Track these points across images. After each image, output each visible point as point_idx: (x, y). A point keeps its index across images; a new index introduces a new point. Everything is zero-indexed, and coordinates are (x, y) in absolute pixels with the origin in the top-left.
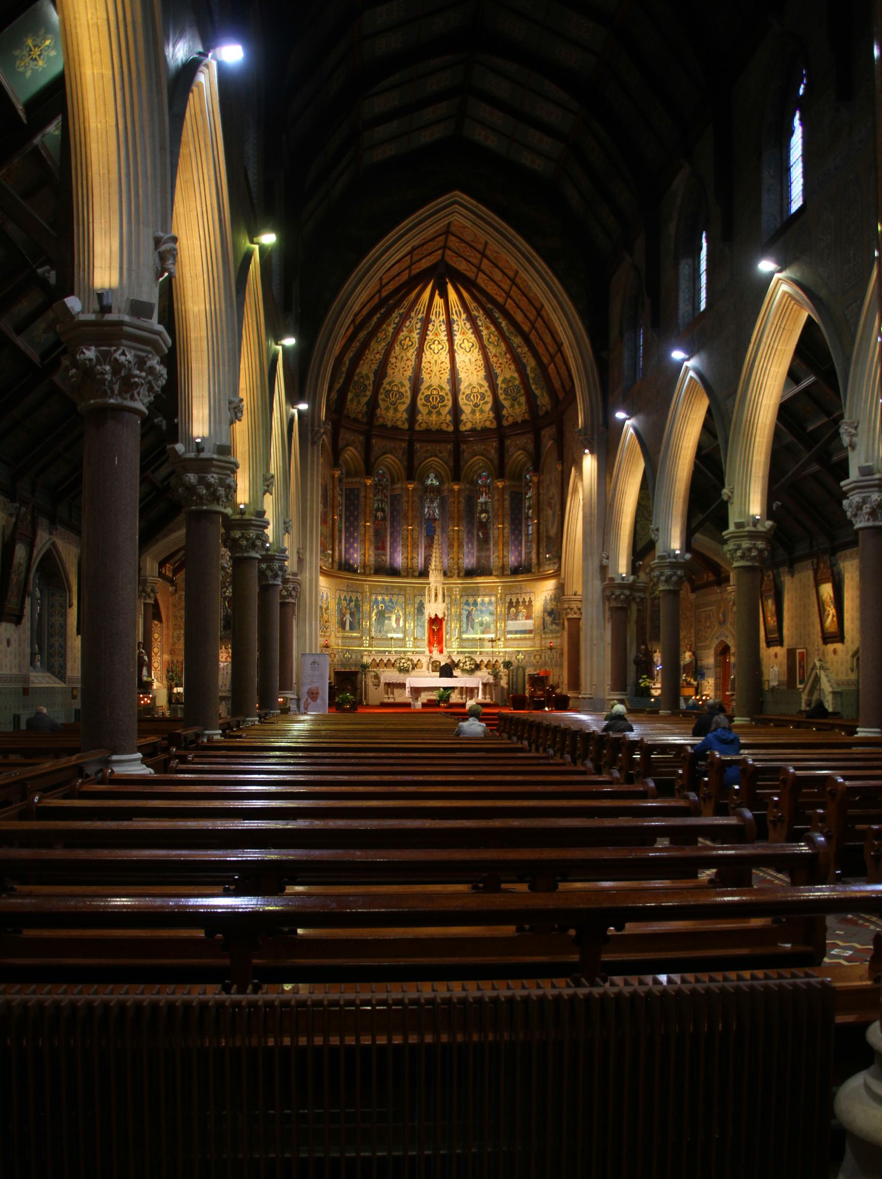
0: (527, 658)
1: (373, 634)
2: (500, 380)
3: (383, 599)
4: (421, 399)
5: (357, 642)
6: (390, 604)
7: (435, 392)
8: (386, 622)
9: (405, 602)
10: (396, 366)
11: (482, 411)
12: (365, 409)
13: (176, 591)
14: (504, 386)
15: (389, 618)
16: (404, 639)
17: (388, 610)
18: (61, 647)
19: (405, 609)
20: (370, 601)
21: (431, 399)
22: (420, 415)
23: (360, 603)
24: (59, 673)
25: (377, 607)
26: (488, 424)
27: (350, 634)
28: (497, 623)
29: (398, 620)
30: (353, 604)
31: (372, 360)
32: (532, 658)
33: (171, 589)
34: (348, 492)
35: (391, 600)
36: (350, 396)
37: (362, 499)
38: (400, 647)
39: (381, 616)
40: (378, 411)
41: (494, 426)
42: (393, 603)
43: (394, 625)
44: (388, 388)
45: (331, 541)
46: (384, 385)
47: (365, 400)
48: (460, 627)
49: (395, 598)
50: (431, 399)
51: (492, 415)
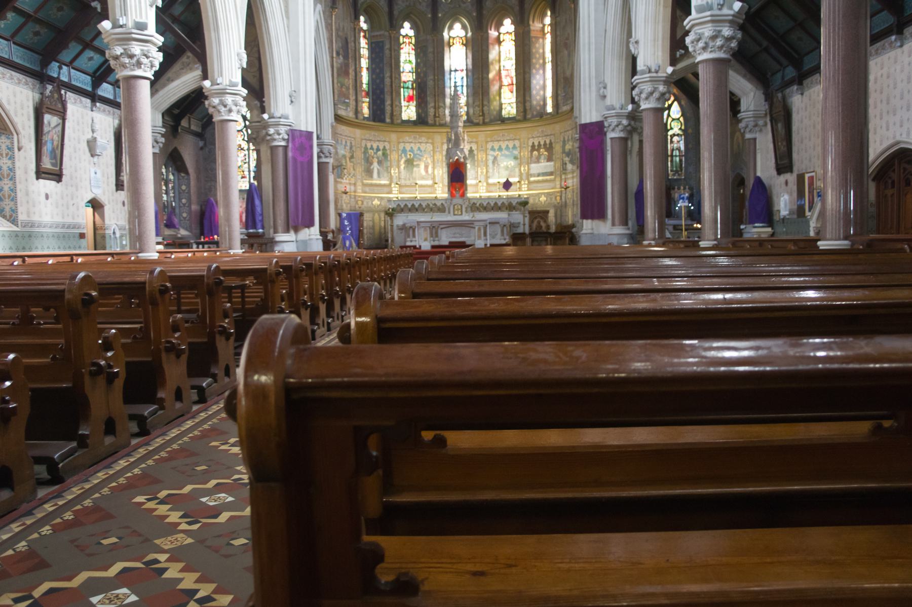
0: (549, 199)
1: (403, 182)
3: (412, 148)
5: (386, 189)
6: (419, 152)
8: (415, 169)
9: (433, 150)
13: (205, 144)
15: (418, 166)
16: (432, 186)
17: (417, 158)
18: (12, 190)
19: (433, 157)
20: (398, 150)
23: (388, 152)
24: (11, 216)
25: (406, 156)
27: (378, 182)
28: (521, 167)
29: (426, 167)
30: (380, 153)
32: (553, 199)
33: (201, 144)
34: (373, 45)
35: (419, 148)
37: (387, 52)
38: (429, 193)
39: (410, 163)
42: (421, 151)
43: (423, 172)
45: (354, 92)
48: (487, 172)
49: (423, 146)
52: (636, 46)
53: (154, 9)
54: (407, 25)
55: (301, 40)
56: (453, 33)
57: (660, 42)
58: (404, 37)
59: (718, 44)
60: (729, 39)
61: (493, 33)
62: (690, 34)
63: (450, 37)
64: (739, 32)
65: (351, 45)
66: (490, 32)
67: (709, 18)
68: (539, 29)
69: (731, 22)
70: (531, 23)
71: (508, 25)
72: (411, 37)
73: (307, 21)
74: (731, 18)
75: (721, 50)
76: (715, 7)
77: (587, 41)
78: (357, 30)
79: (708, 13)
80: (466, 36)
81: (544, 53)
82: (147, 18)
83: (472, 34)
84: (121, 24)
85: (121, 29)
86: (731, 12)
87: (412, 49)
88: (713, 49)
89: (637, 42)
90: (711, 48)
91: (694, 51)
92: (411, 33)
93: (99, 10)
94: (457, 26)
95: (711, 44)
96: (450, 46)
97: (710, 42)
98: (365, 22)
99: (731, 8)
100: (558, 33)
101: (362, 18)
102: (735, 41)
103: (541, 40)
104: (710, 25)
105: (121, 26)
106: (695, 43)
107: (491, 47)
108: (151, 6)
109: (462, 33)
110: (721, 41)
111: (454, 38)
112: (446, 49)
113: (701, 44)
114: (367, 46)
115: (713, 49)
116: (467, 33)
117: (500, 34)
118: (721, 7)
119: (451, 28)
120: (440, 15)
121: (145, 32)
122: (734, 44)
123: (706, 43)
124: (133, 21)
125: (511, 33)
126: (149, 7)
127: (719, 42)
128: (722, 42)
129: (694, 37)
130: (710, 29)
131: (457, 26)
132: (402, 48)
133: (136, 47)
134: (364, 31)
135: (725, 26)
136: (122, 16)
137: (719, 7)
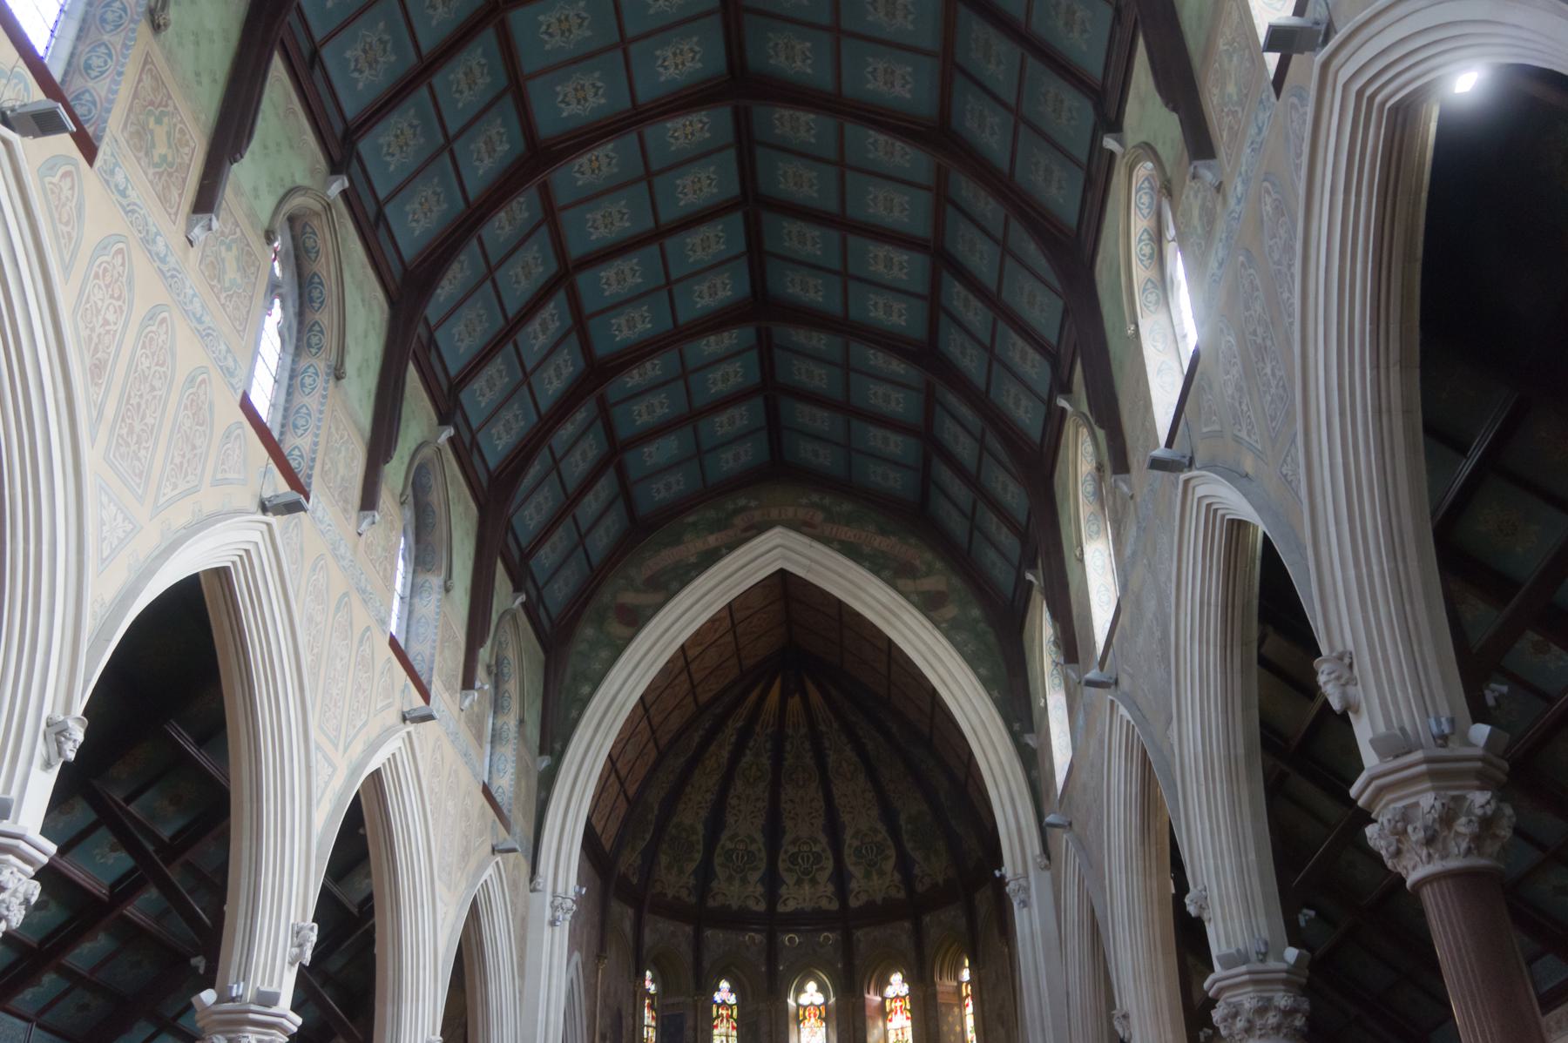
2: (902, 819)
4: (784, 861)
7: (805, 848)
10: (740, 811)
11: (881, 873)
12: (692, 881)
14: (909, 827)
21: (800, 861)
22: (785, 887)
26: (893, 893)
31: (700, 803)
36: (664, 860)
40: (714, 884)
41: (902, 895)
44: (730, 845)
46: (722, 842)
47: (692, 866)
50: (800, 861)
51: (897, 876)
52: (1124, 1023)
53: (295, 969)
54: (724, 985)
55: (541, 1016)
56: (804, 999)
57: (1167, 1016)
58: (719, 1006)
59: (1270, 1022)
60: (1288, 1013)
61: (873, 998)
62: (1217, 1005)
63: (799, 1006)
64: (1304, 999)
65: (627, 1022)
66: (867, 996)
67: (1246, 977)
68: (951, 990)
69: (1285, 982)
70: (937, 979)
71: (897, 985)
72: (731, 1006)
73: (554, 981)
74: (1284, 975)
75: (1278, 1033)
76: (1253, 957)
77: (1036, 1011)
78: (639, 993)
79: (1243, 968)
80: (825, 1003)
81: (963, 1031)
82: (280, 985)
83: (837, 1000)
84: (234, 995)
85: (231, 1004)
86: (1283, 966)
87: (733, 1028)
88: (1263, 1032)
89: (1126, 1017)
90: (1260, 1029)
91: (1231, 1035)
92: (732, 999)
93: (201, 971)
94: (811, 986)
95: (1259, 1023)
96: (799, 1022)
97: (1257, 1019)
98: (653, 981)
99: (1281, 959)
100: (985, 996)
101: (648, 974)
102: (1299, 1015)
103: (956, 1010)
104: (1250, 989)
105: (233, 1000)
106: (1229, 1020)
107: (869, 1023)
108: (292, 964)
109: (819, 999)
110: (1275, 1016)
111: (805, 1007)
112: (792, 1027)
113: (1240, 1024)
114: (654, 1024)
115: (1263, 1032)
116: (827, 998)
117: (884, 999)
118: (1263, 957)
119: (800, 990)
120: (781, 968)
121: (273, 1010)
122: (1299, 1022)
123: (1249, 1021)
124: (255, 990)
125: (904, 998)
126: (287, 965)
127: (1272, 1019)
128: (1278, 1016)
129: (1226, 1011)
130: (1252, 995)
131: (811, 986)
132: (716, 1027)
133: (250, 1035)
134: (651, 997)
135: (1279, 990)
136: (237, 982)
137: (1261, 957)
